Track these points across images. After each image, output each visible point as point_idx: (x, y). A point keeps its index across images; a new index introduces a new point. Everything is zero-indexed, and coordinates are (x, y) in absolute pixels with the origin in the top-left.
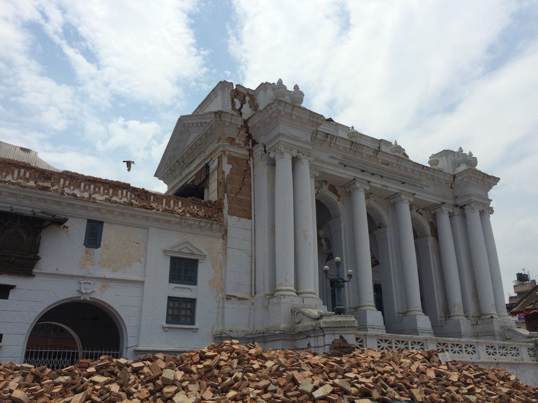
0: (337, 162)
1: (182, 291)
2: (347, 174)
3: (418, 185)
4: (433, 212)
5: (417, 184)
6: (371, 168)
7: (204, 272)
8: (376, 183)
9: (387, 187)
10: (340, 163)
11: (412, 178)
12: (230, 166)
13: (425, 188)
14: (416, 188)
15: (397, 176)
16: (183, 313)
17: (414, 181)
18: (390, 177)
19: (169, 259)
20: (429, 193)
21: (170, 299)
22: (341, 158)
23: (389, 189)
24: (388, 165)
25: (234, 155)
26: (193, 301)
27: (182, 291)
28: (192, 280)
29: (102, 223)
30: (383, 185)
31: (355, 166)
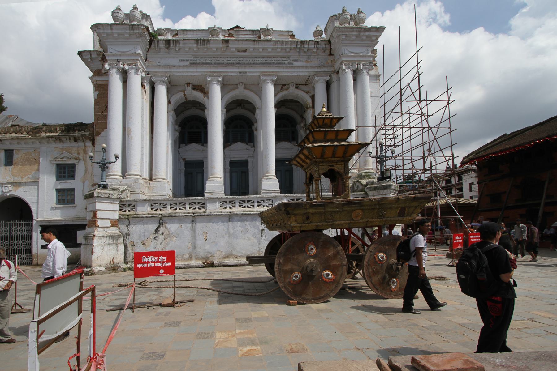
1: (66, 184)
2: (196, 73)
3: (286, 62)
5: (284, 62)
6: (227, 59)
7: (80, 171)
8: (232, 72)
9: (246, 72)
10: (191, 64)
12: (97, 92)
14: (284, 65)
19: (55, 165)
20: (299, 67)
22: (192, 58)
23: (248, 74)
24: (245, 51)
25: (101, 83)
26: (73, 190)
27: (66, 184)
28: (72, 177)
30: (239, 72)
31: (208, 61)
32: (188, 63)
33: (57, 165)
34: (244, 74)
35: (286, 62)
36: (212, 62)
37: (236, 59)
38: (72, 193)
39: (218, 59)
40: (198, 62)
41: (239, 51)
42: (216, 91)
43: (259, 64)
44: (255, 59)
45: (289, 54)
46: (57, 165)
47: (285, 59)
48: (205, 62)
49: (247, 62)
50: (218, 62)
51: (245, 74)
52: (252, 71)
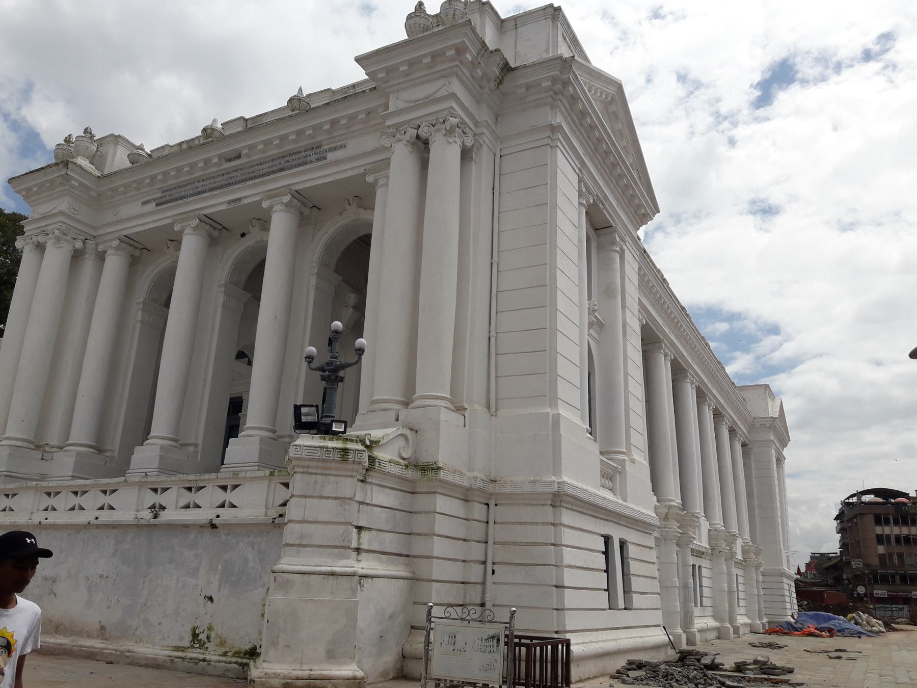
0: (152, 206)
5: (309, 158)
6: (212, 181)
9: (239, 200)
10: (157, 205)
11: (299, 153)
15: (263, 166)
23: (246, 201)
24: (239, 157)
30: (230, 202)
36: (188, 193)
37: (228, 176)
40: (167, 198)
41: (229, 160)
42: (191, 246)
45: (318, 139)
49: (244, 177)
50: (198, 190)
52: (249, 193)
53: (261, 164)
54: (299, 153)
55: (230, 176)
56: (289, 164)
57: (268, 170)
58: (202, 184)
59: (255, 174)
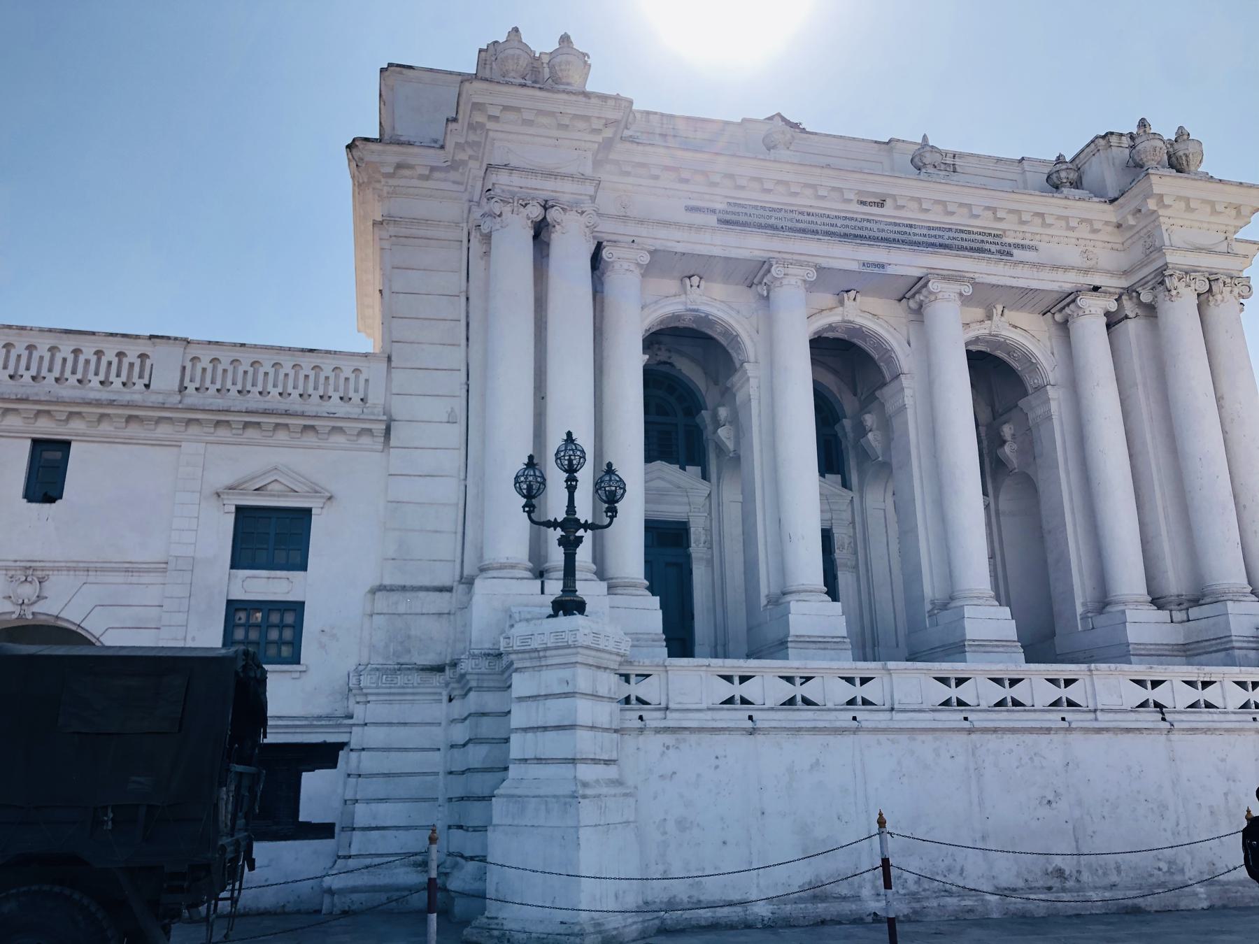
3: (993, 248)
4: (1058, 317)
5: (987, 246)
9: (882, 266)
13: (1015, 252)
16: (274, 635)
17: (980, 238)
18: (892, 236)
21: (233, 606)
23: (890, 270)
24: (881, 204)
26: (297, 608)
29: (65, 445)
31: (772, 221)
32: (712, 220)
33: (242, 512)
34: (876, 270)
35: (993, 248)
36: (784, 223)
37: (853, 223)
38: (289, 618)
39: (800, 217)
40: (742, 218)
43: (918, 244)
44: (908, 230)
46: (240, 510)
47: (990, 239)
48: (763, 221)
51: (881, 271)
53: (911, 226)
54: (969, 232)
55: (860, 225)
56: (956, 242)
57: (925, 239)
58: (806, 218)
59: (904, 237)
